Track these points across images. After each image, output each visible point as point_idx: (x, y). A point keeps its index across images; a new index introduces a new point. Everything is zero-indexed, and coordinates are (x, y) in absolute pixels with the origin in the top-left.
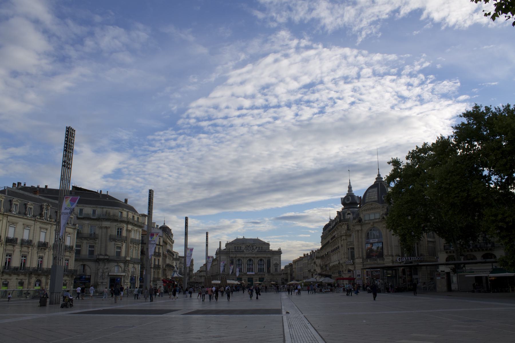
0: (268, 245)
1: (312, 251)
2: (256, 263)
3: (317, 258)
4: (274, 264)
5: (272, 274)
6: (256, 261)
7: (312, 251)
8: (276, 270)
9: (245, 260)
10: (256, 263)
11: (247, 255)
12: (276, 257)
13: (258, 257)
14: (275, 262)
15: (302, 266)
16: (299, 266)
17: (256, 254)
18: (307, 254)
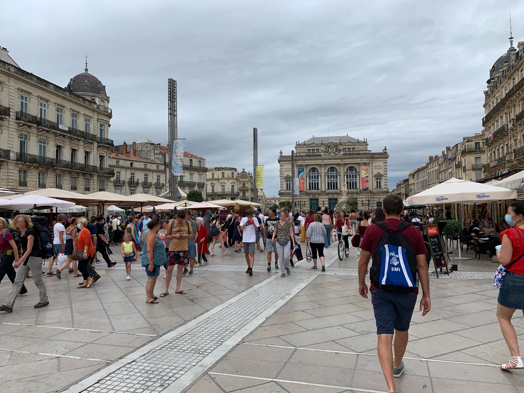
0: (365, 143)
1: (448, 149)
2: (342, 174)
3: (464, 153)
4: (375, 176)
5: (371, 192)
6: (342, 170)
7: (448, 149)
8: (379, 185)
9: (323, 169)
10: (342, 174)
11: (326, 162)
12: (378, 163)
13: (345, 164)
14: (375, 172)
15: (426, 178)
16: (420, 180)
17: (342, 159)
18: (436, 157)
